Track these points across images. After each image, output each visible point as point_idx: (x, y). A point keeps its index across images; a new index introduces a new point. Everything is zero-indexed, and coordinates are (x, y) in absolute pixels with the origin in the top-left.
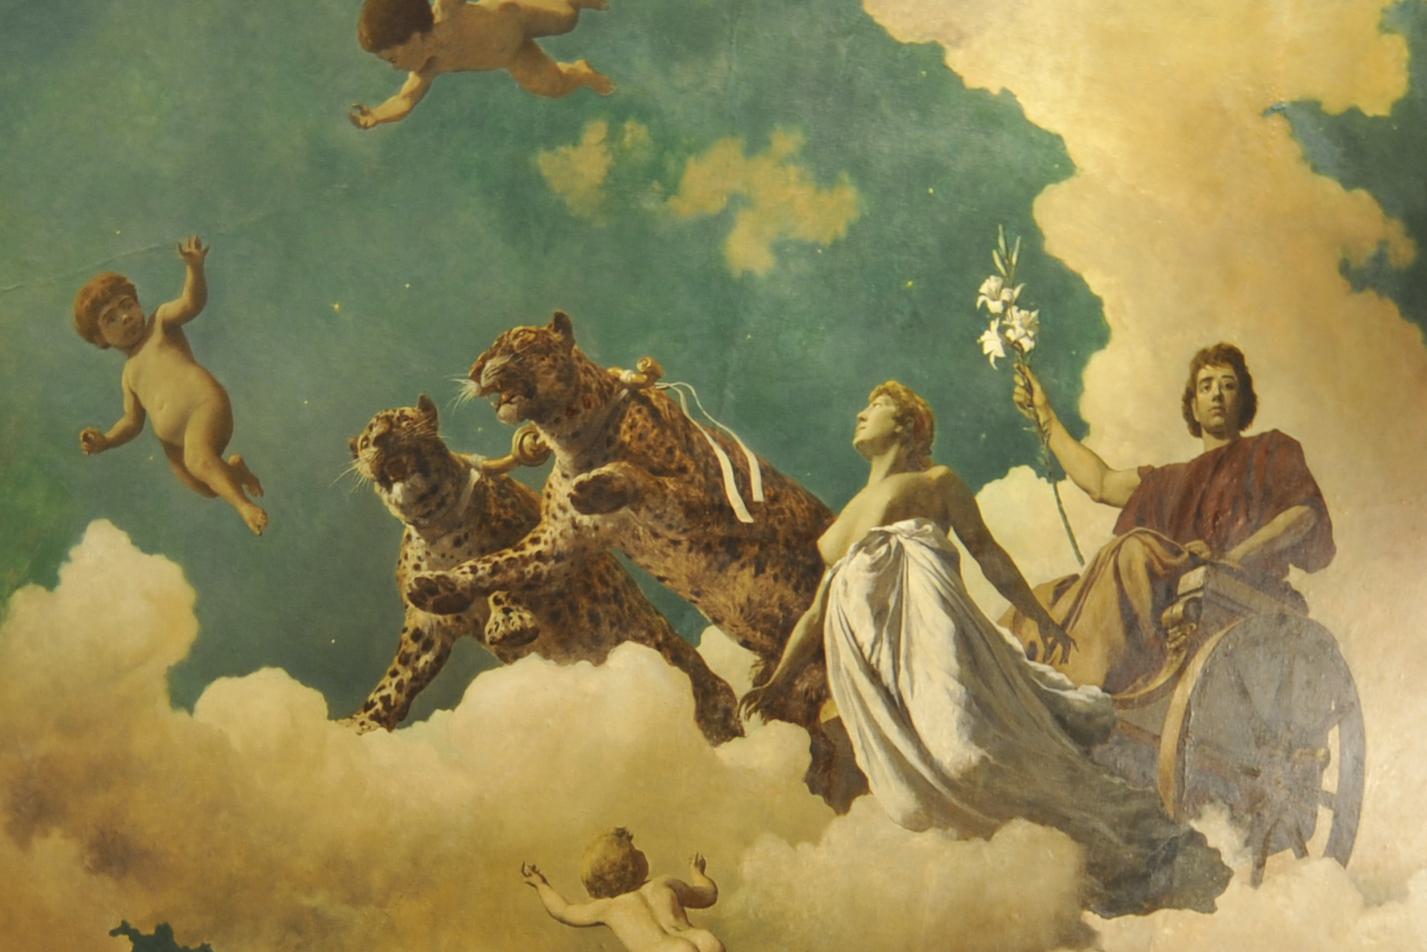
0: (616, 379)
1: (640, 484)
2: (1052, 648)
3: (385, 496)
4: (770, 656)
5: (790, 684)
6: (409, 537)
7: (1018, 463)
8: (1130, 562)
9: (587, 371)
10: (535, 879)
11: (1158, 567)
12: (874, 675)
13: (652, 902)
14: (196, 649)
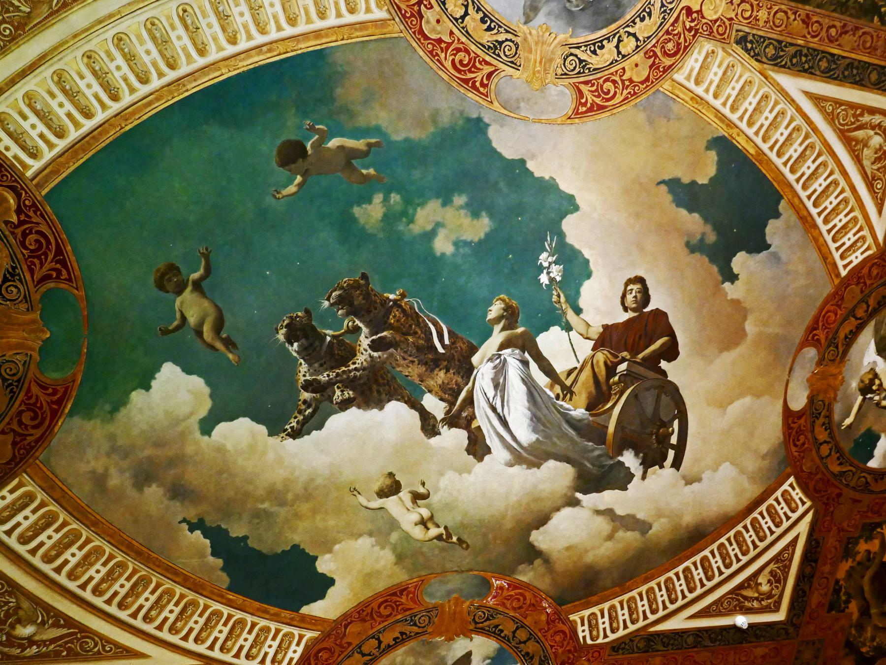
0: (388, 298)
1: (398, 339)
2: (566, 395)
3: (290, 348)
4: (452, 404)
5: (460, 414)
6: (301, 364)
7: (553, 325)
8: (598, 362)
9: (375, 295)
10: (355, 493)
11: (609, 362)
12: (494, 409)
13: (403, 499)
14: (211, 411)
